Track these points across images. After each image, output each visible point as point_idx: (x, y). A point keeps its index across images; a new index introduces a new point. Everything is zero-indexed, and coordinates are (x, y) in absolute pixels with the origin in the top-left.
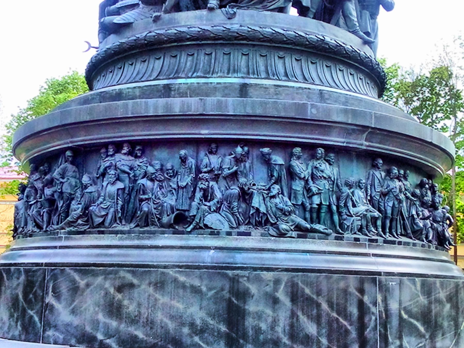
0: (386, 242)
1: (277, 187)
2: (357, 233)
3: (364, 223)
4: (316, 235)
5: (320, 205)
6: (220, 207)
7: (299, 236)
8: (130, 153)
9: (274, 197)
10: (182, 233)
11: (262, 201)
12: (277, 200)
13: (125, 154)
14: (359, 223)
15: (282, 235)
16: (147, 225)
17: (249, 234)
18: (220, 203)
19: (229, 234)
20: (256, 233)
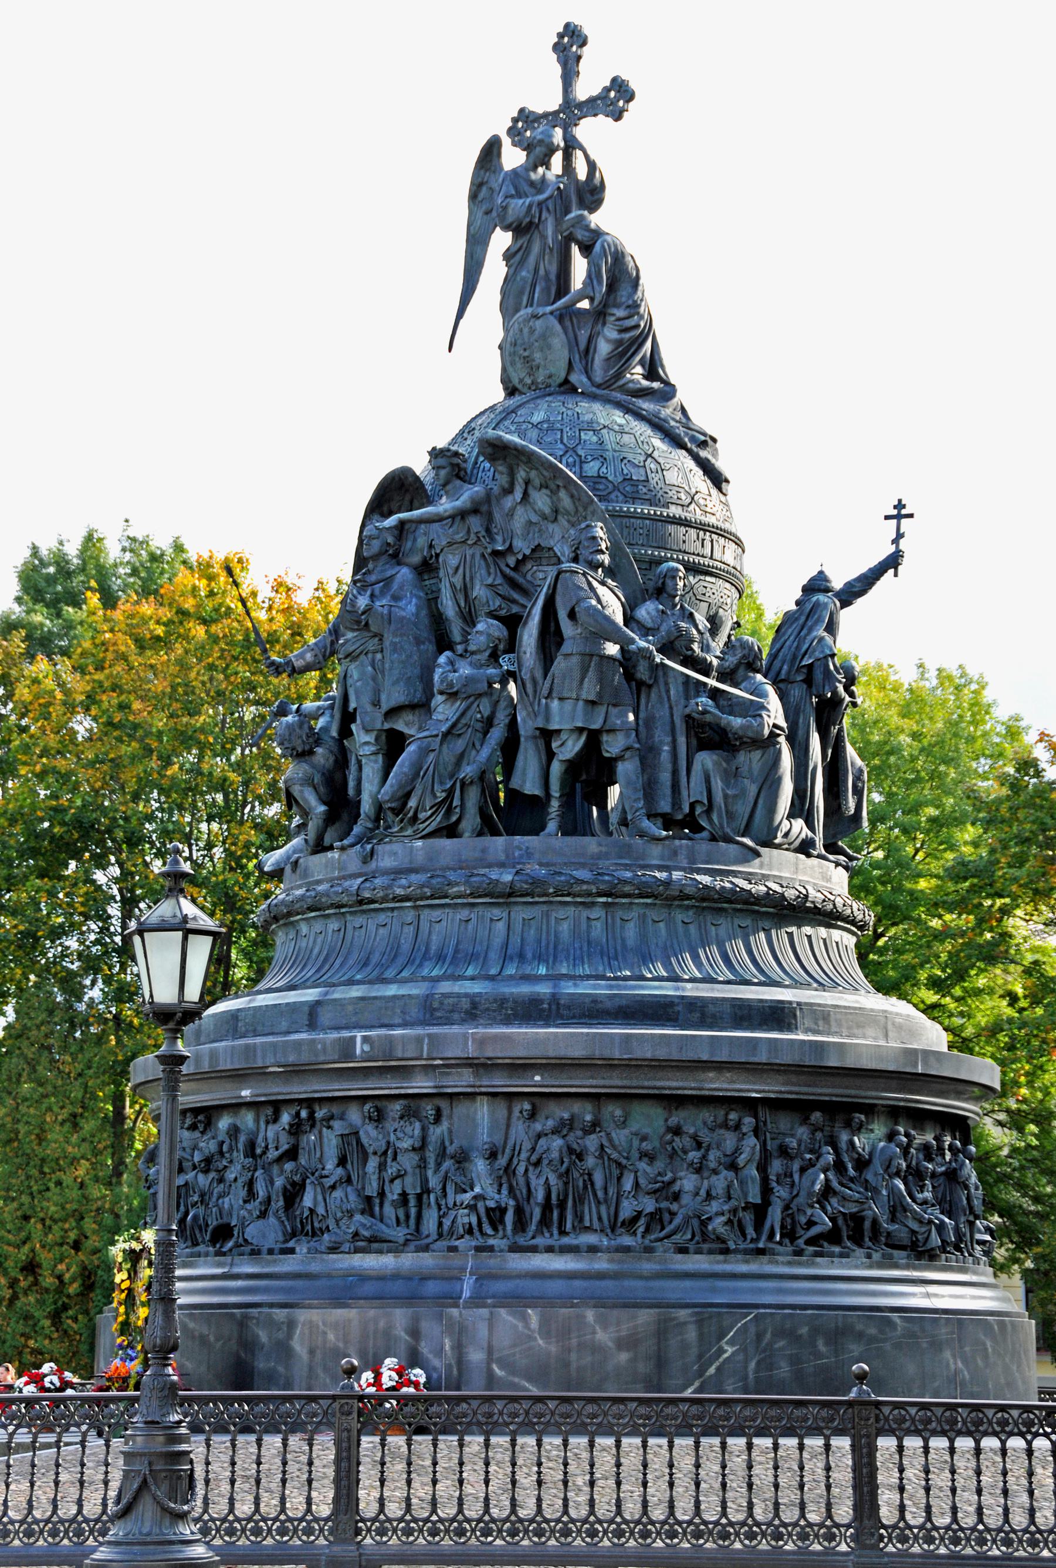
0: (515, 1248)
1: (340, 1171)
2: (467, 1237)
3: (474, 1220)
4: (385, 1245)
5: (404, 1195)
6: (266, 1210)
7: (357, 1251)
8: (193, 1127)
9: (333, 1187)
10: (224, 1254)
11: (320, 1198)
12: (338, 1194)
13: (188, 1129)
14: (466, 1220)
15: (334, 1249)
16: (197, 1244)
17: (292, 1251)
18: (268, 1201)
19: (271, 1252)
20: (302, 1248)
